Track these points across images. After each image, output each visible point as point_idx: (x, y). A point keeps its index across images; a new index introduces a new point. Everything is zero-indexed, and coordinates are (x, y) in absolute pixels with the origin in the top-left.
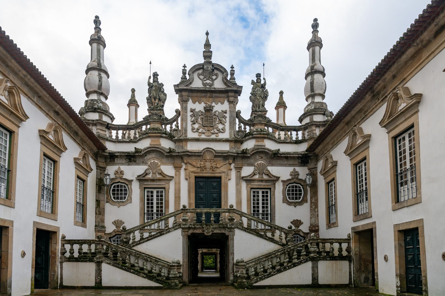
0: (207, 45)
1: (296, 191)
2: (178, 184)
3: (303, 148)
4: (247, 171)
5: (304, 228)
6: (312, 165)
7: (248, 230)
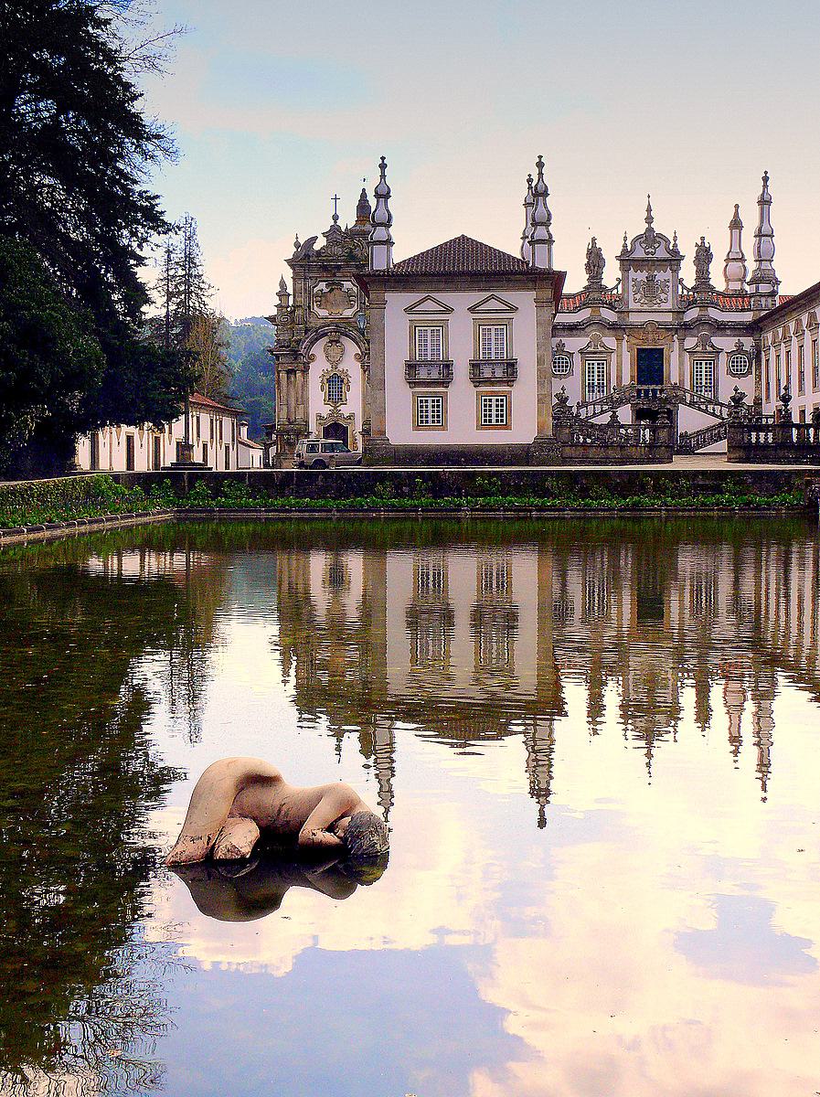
0: (649, 210)
1: (741, 362)
2: (620, 356)
3: (748, 317)
4: (690, 342)
5: (749, 401)
6: (757, 337)
7: (692, 404)
